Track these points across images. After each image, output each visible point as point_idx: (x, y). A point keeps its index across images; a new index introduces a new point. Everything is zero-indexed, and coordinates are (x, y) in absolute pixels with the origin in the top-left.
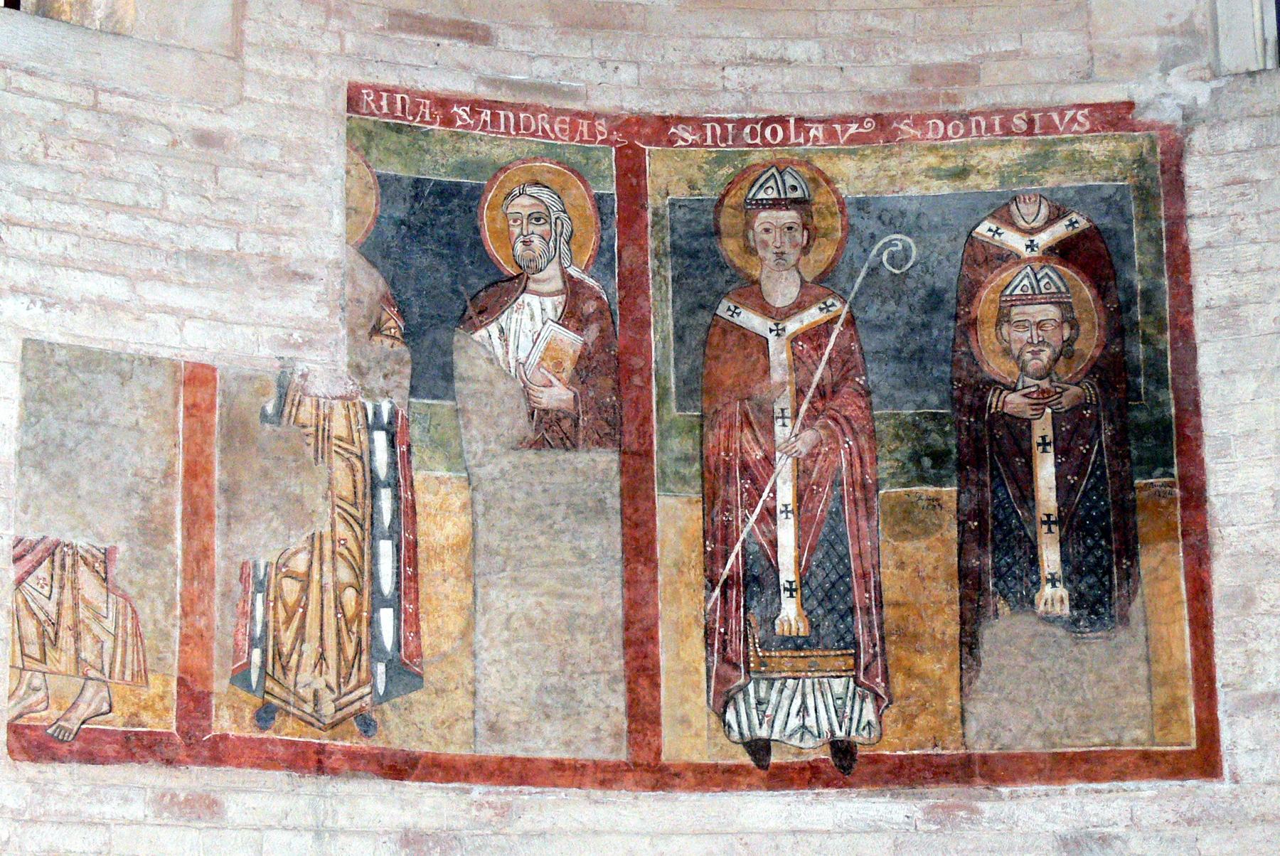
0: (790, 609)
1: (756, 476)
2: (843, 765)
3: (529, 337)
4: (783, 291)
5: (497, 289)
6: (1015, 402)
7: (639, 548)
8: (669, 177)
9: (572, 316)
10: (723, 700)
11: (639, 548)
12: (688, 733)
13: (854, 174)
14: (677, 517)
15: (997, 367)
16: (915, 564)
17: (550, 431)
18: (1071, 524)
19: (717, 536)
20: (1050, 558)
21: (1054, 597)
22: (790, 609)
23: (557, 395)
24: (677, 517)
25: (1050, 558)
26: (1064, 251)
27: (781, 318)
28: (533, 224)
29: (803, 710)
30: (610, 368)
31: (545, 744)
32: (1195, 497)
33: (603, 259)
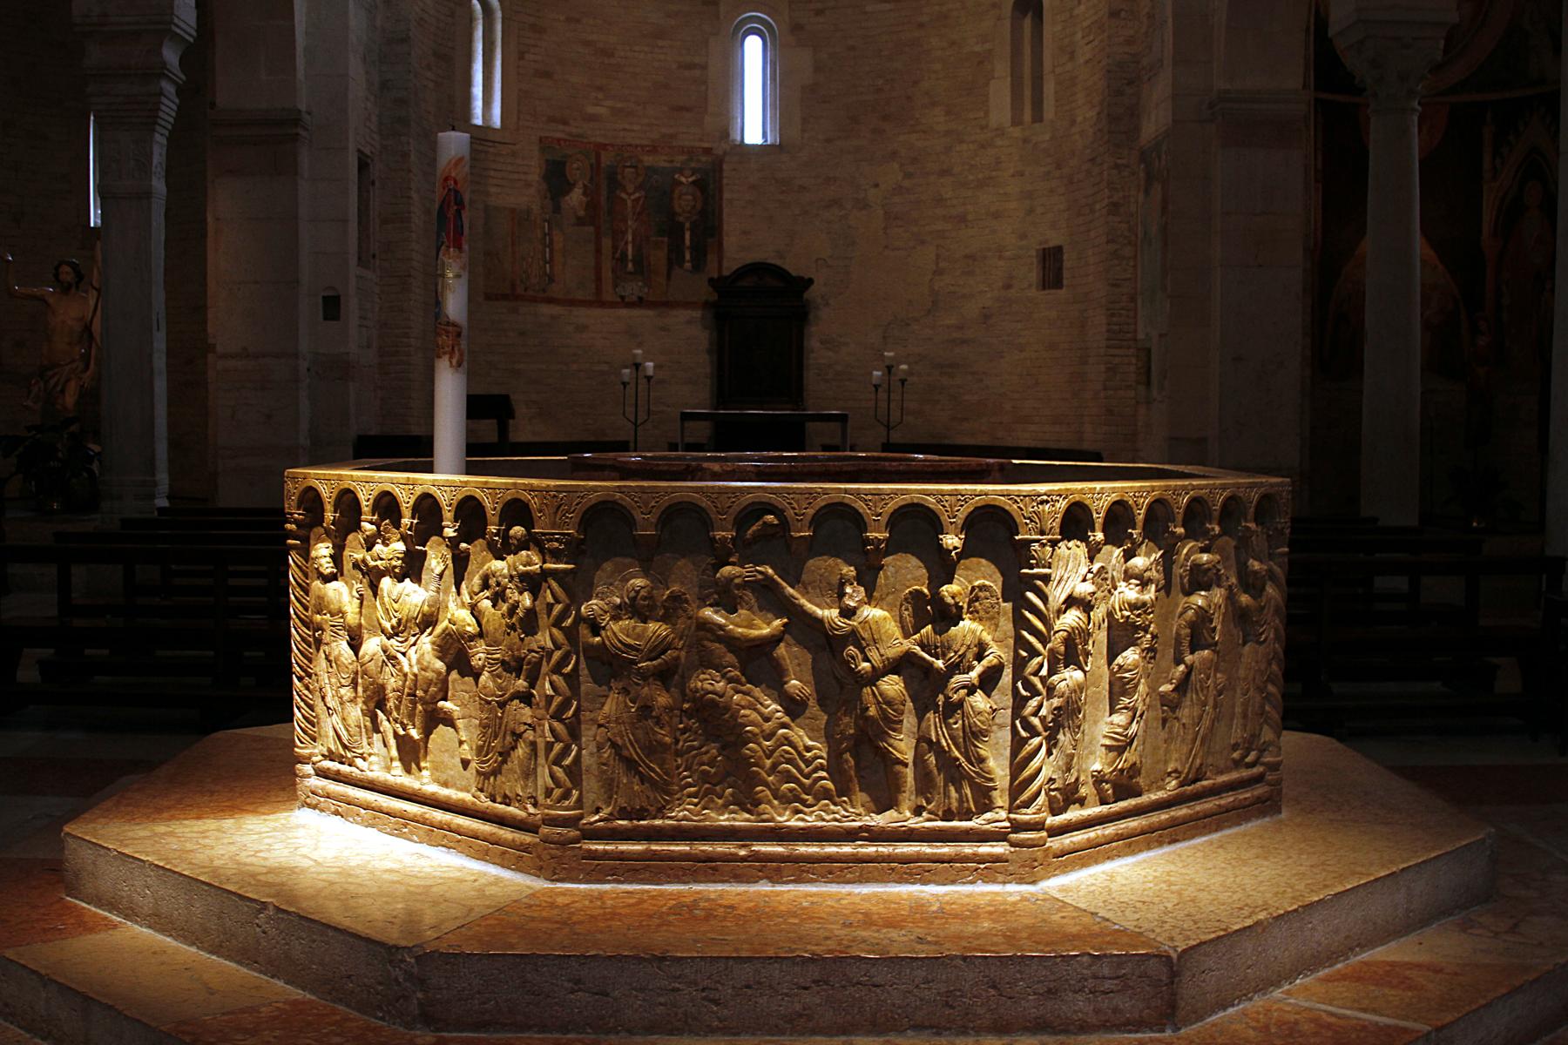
0: (630, 265)
1: (624, 233)
2: (640, 303)
3: (576, 198)
4: (630, 188)
5: (570, 187)
6: (681, 219)
7: (598, 251)
8: (607, 159)
9: (585, 194)
10: (616, 286)
11: (598, 251)
12: (608, 296)
13: (648, 160)
14: (607, 243)
15: (678, 210)
16: (658, 257)
17: (580, 222)
18: (693, 248)
19: (615, 248)
20: (688, 257)
21: (688, 265)
22: (630, 265)
23: (582, 213)
24: (607, 243)
25: (688, 257)
26: (693, 183)
27: (630, 197)
28: (577, 169)
29: (633, 289)
30: (592, 206)
31: (579, 295)
32: (721, 244)
33: (591, 179)
